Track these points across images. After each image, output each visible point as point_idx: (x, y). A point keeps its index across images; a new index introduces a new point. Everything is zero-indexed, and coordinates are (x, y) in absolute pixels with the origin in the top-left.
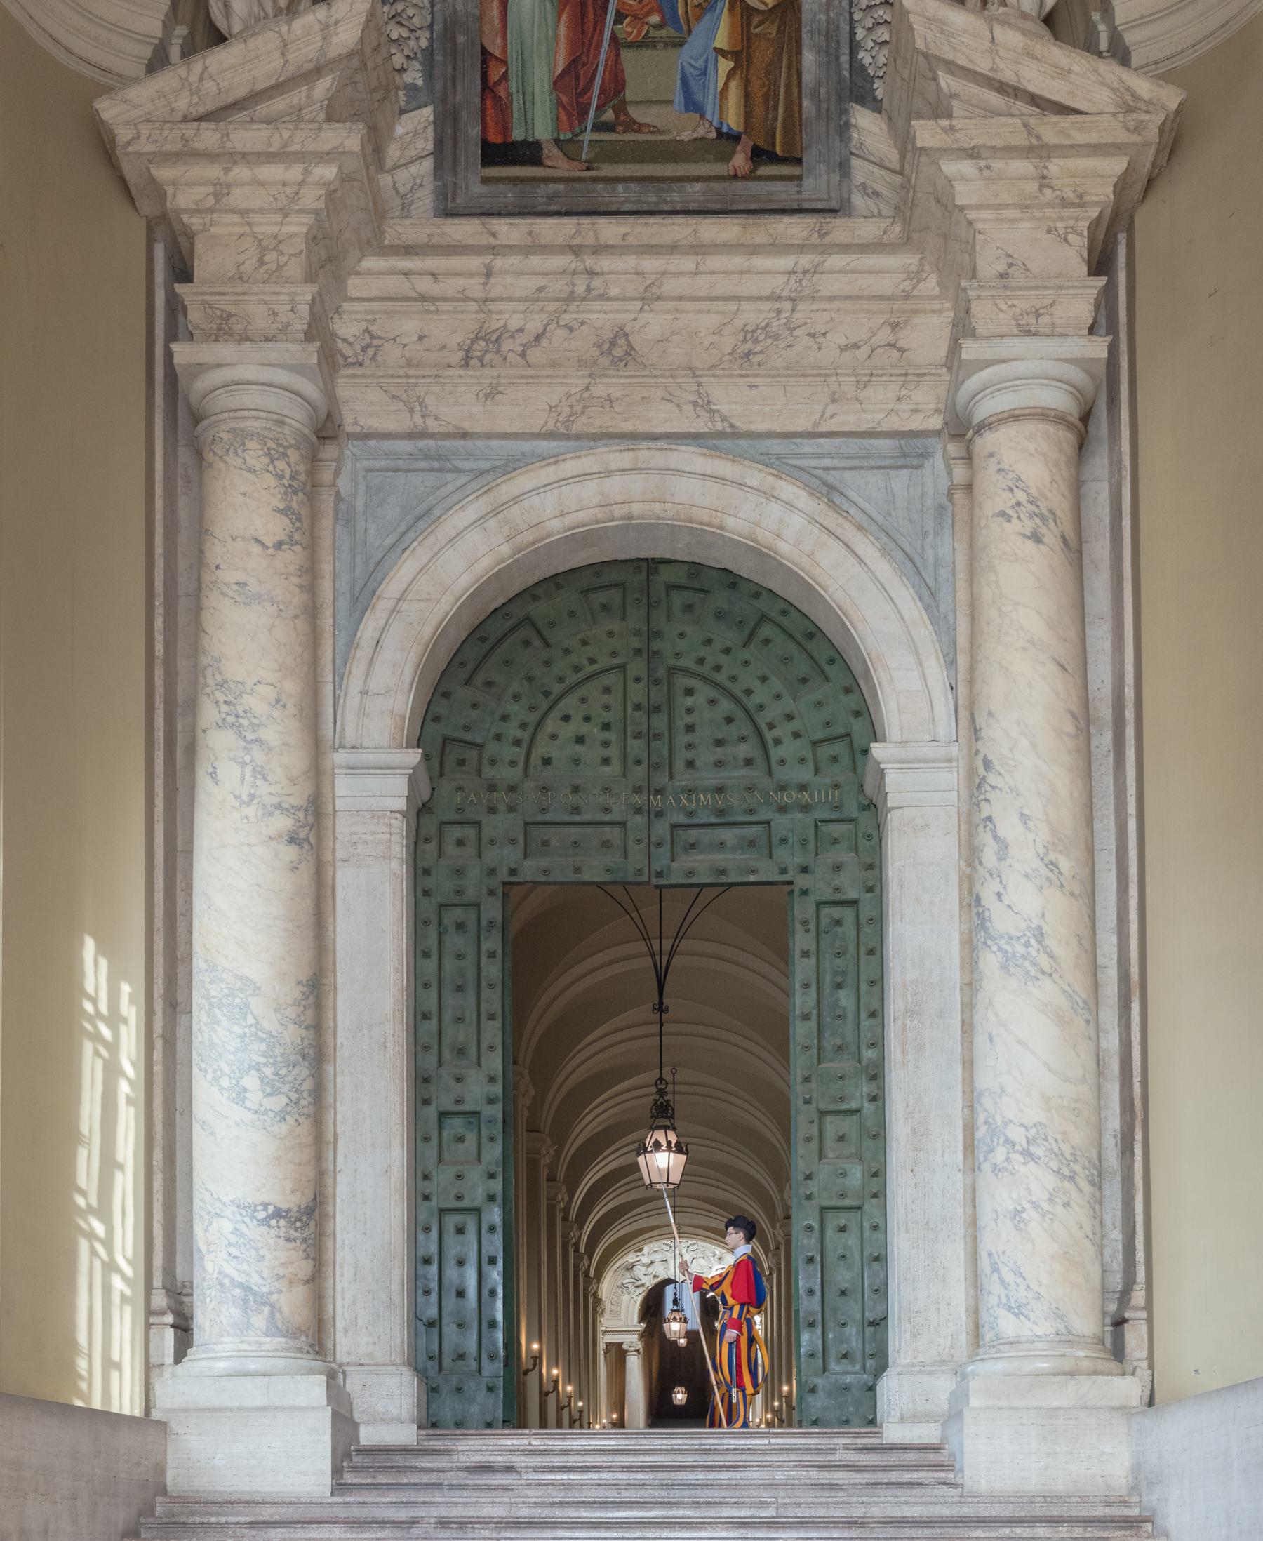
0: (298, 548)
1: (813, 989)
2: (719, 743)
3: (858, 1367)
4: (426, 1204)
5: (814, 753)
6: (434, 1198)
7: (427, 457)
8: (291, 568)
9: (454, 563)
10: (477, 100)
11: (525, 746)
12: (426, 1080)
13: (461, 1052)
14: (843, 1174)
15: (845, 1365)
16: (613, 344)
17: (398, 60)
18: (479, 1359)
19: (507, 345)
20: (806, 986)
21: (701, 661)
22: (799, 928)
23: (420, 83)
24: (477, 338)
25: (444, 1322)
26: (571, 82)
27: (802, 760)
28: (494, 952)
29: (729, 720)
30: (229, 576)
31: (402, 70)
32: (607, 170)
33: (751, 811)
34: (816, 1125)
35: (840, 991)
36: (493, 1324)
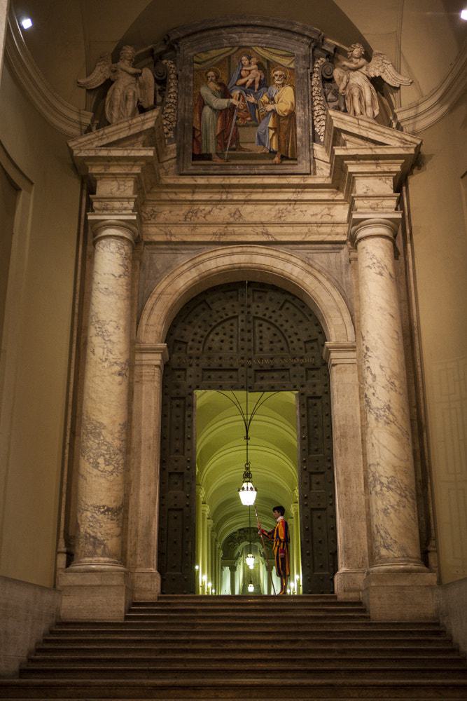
0: (126, 277)
2: (271, 342)
5: (305, 346)
7: (172, 249)
8: (124, 284)
9: (180, 279)
10: (191, 142)
11: (203, 342)
12: (164, 462)
16: (235, 214)
17: (166, 130)
19: (199, 214)
21: (265, 315)
23: (172, 137)
24: (189, 212)
26: (222, 137)
27: (301, 348)
29: (275, 335)
30: (102, 286)
31: (167, 134)
32: (233, 162)
33: (283, 366)
34: (308, 479)
35: (316, 430)
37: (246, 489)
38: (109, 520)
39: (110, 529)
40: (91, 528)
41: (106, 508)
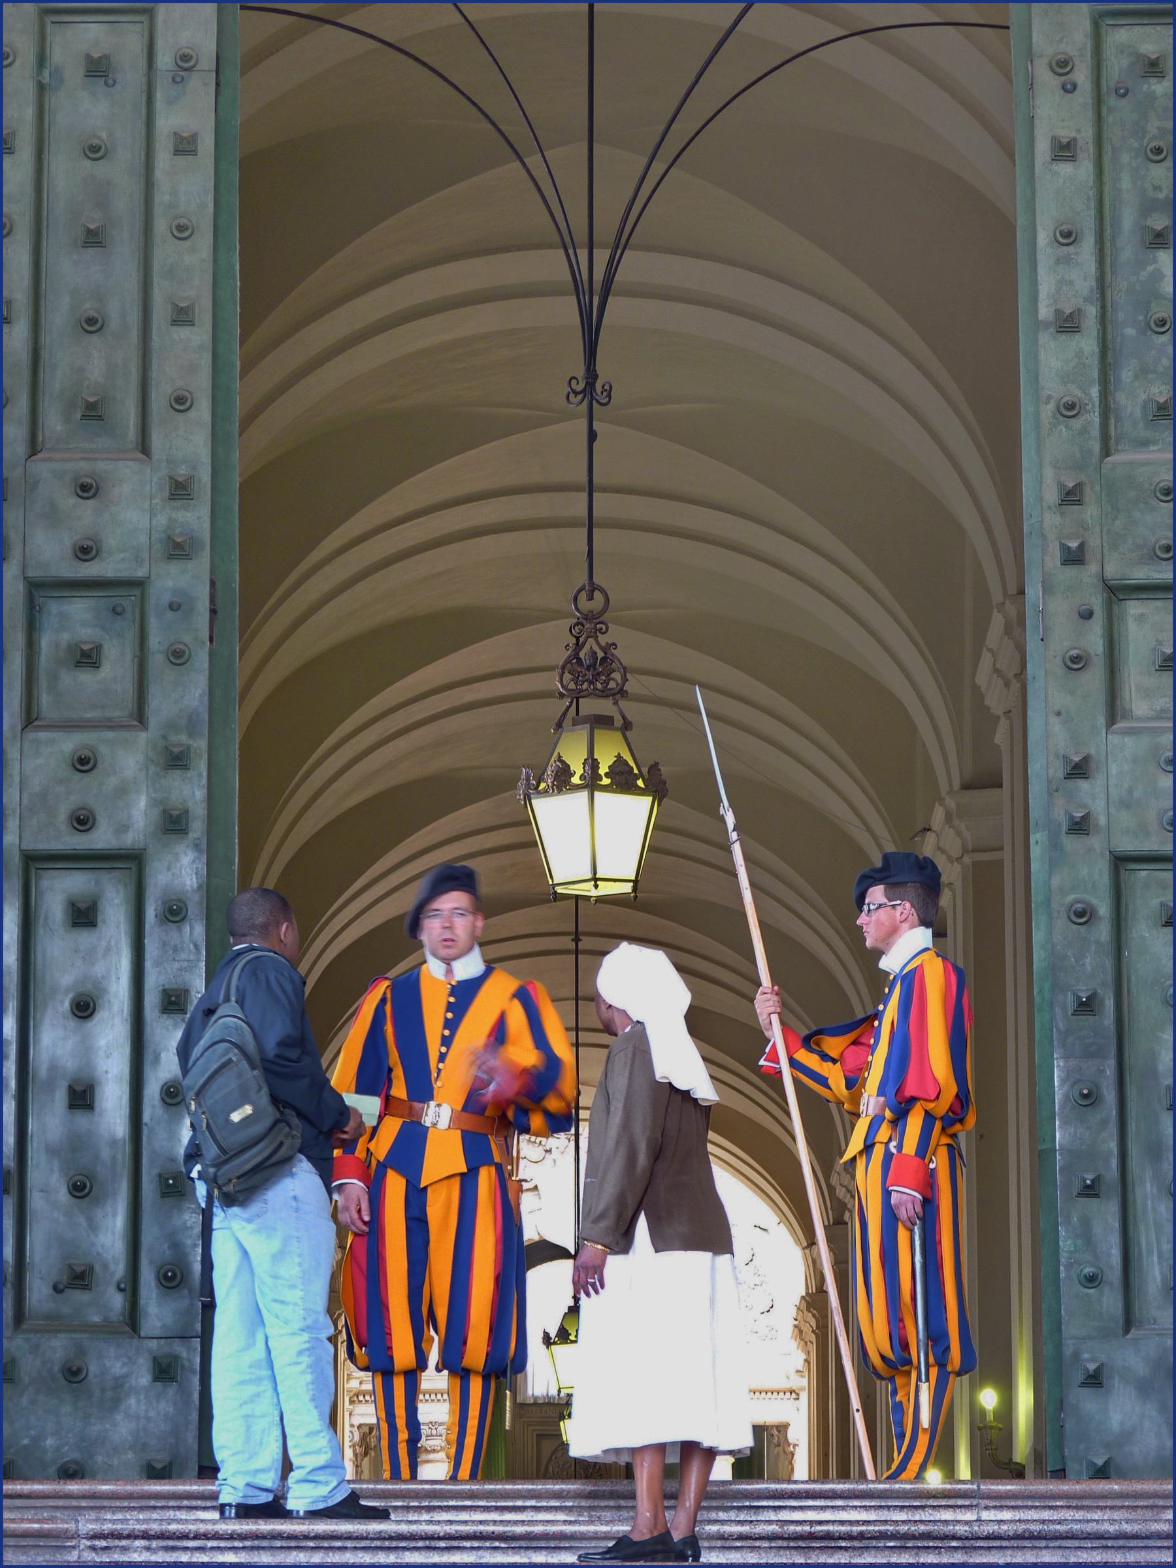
1: (1087, 249)
13: (94, 413)
18: (131, 1286)
20: (1068, 237)
22: (1046, 79)
25: (35, 1177)
28: (194, 138)
34: (1097, 626)
37: (576, 780)
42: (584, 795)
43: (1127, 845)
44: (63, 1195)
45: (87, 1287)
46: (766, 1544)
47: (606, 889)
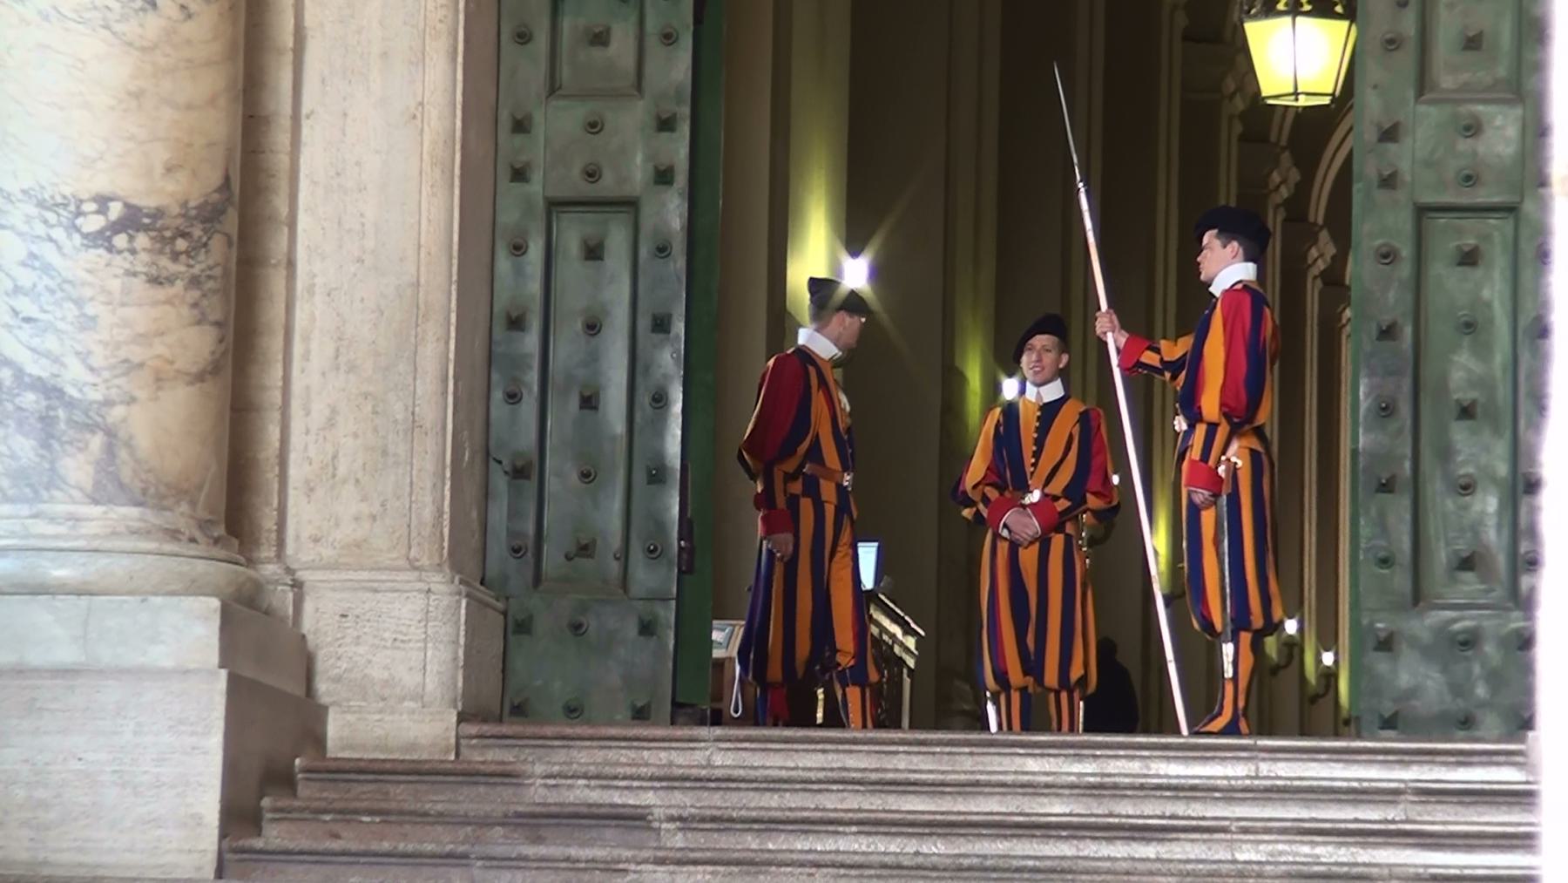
3: (1499, 593)
4: (518, 187)
6: (537, 177)
14: (1473, 129)
15: (1470, 583)
18: (624, 556)
36: (657, 475)
38: (138, 283)
39: (142, 338)
40: (26, 332)
41: (116, 210)
42: (1287, 20)
43: (1429, 198)
44: (574, 477)
45: (591, 556)
46: (1067, 792)
47: (1303, 101)
